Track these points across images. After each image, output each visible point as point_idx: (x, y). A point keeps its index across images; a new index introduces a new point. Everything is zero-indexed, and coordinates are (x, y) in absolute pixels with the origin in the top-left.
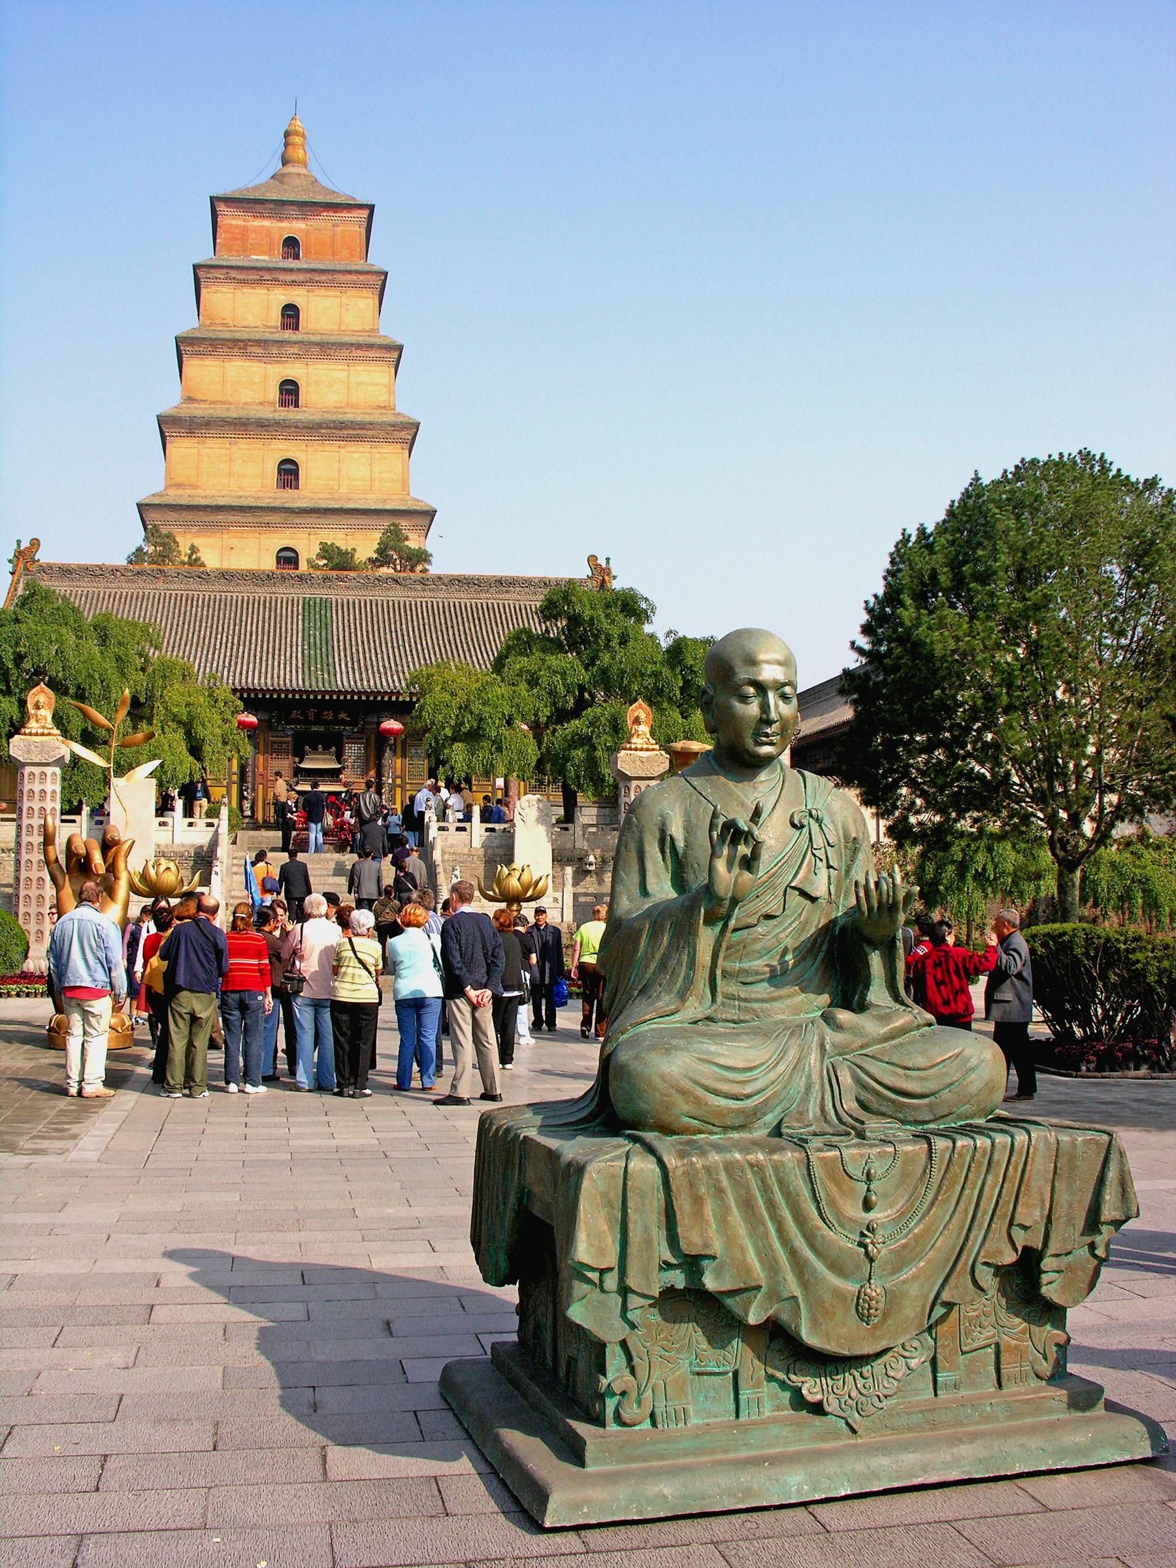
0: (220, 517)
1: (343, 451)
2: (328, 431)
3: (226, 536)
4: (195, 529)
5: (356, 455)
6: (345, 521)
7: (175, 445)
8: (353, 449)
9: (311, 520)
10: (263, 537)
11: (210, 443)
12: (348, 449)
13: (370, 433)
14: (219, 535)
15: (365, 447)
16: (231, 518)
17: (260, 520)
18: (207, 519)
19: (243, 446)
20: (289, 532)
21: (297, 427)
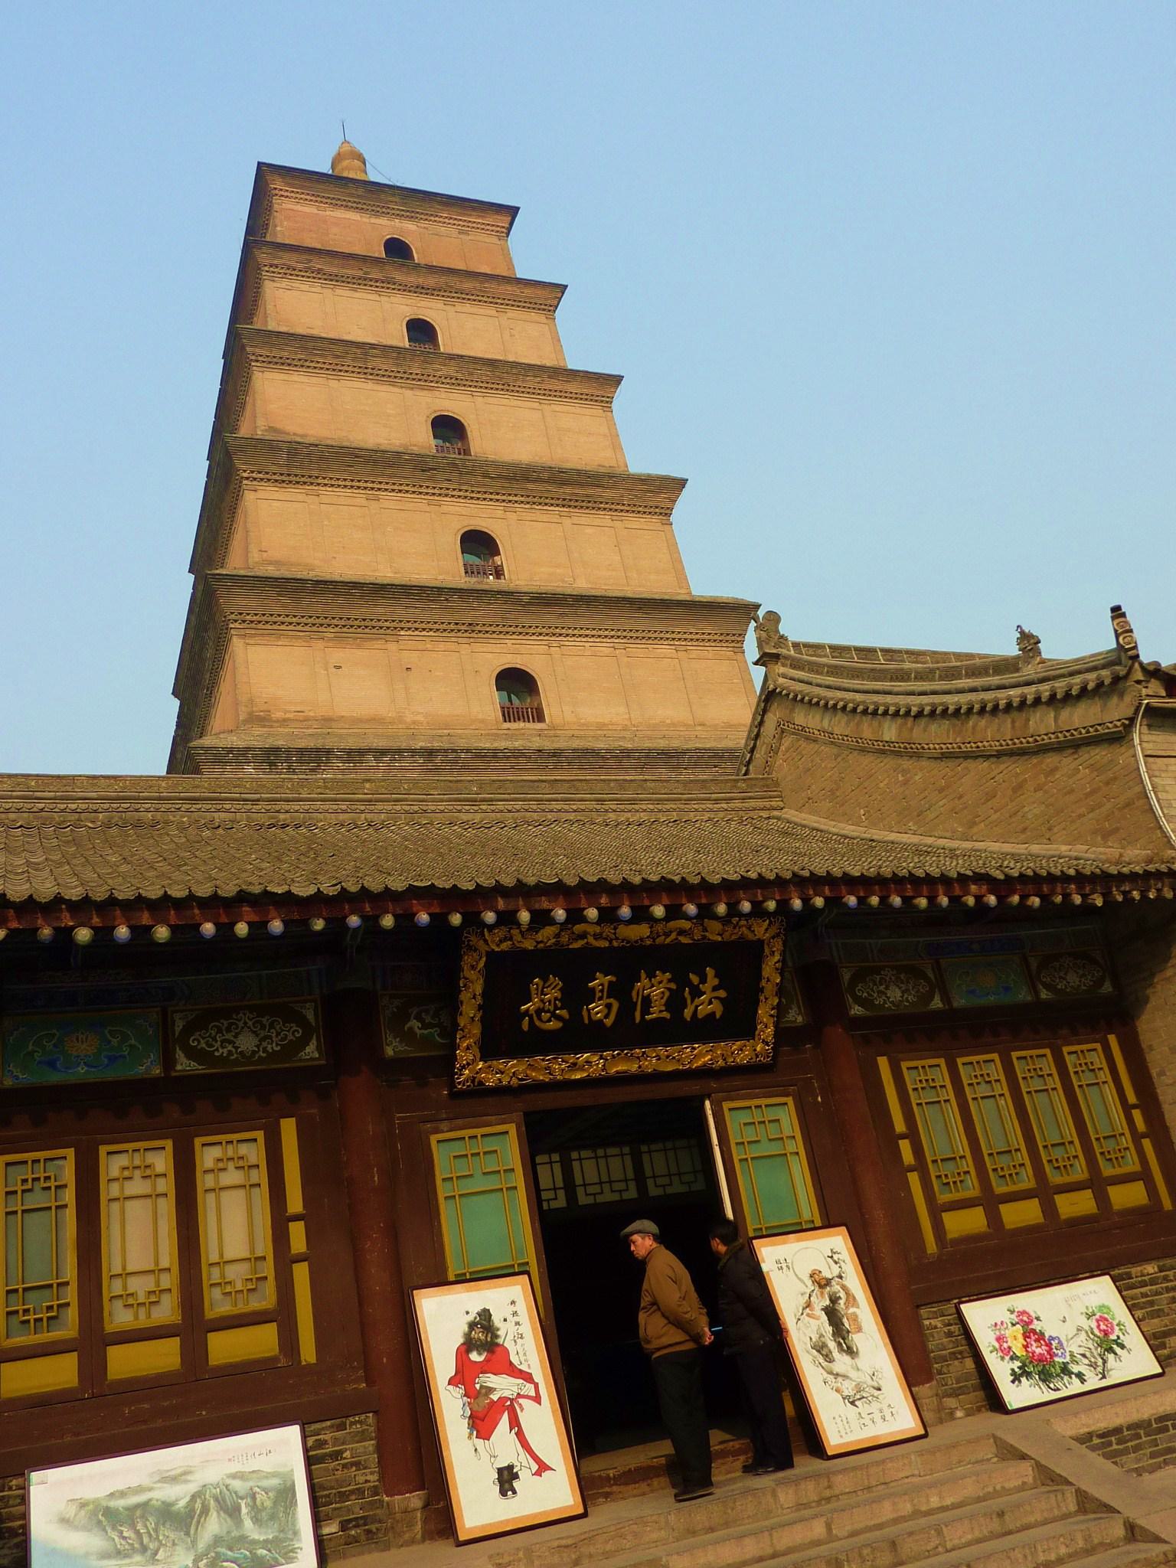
0: (381, 609)
1: (567, 521)
2: (540, 487)
3: (392, 647)
4: (329, 633)
5: (589, 530)
6: (609, 624)
7: (260, 494)
8: (583, 520)
9: (550, 618)
10: (465, 649)
11: (328, 495)
12: (575, 520)
13: (608, 494)
14: (378, 644)
15: (604, 519)
16: (400, 612)
17: (457, 617)
18: (355, 613)
19: (392, 505)
20: (509, 642)
21: (485, 476)
